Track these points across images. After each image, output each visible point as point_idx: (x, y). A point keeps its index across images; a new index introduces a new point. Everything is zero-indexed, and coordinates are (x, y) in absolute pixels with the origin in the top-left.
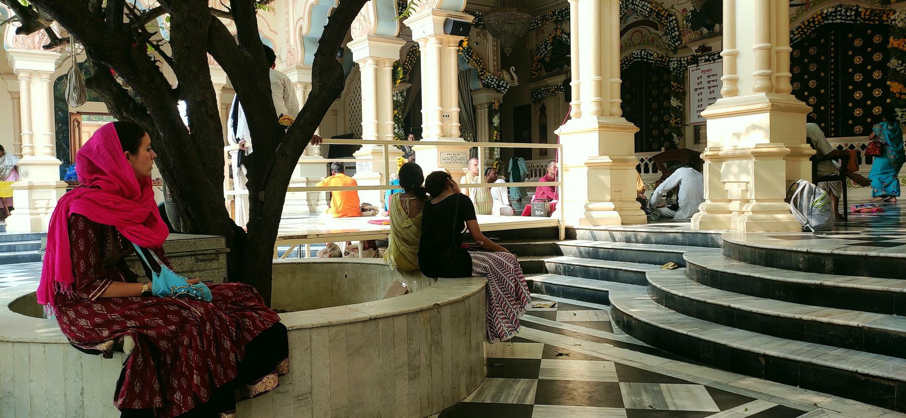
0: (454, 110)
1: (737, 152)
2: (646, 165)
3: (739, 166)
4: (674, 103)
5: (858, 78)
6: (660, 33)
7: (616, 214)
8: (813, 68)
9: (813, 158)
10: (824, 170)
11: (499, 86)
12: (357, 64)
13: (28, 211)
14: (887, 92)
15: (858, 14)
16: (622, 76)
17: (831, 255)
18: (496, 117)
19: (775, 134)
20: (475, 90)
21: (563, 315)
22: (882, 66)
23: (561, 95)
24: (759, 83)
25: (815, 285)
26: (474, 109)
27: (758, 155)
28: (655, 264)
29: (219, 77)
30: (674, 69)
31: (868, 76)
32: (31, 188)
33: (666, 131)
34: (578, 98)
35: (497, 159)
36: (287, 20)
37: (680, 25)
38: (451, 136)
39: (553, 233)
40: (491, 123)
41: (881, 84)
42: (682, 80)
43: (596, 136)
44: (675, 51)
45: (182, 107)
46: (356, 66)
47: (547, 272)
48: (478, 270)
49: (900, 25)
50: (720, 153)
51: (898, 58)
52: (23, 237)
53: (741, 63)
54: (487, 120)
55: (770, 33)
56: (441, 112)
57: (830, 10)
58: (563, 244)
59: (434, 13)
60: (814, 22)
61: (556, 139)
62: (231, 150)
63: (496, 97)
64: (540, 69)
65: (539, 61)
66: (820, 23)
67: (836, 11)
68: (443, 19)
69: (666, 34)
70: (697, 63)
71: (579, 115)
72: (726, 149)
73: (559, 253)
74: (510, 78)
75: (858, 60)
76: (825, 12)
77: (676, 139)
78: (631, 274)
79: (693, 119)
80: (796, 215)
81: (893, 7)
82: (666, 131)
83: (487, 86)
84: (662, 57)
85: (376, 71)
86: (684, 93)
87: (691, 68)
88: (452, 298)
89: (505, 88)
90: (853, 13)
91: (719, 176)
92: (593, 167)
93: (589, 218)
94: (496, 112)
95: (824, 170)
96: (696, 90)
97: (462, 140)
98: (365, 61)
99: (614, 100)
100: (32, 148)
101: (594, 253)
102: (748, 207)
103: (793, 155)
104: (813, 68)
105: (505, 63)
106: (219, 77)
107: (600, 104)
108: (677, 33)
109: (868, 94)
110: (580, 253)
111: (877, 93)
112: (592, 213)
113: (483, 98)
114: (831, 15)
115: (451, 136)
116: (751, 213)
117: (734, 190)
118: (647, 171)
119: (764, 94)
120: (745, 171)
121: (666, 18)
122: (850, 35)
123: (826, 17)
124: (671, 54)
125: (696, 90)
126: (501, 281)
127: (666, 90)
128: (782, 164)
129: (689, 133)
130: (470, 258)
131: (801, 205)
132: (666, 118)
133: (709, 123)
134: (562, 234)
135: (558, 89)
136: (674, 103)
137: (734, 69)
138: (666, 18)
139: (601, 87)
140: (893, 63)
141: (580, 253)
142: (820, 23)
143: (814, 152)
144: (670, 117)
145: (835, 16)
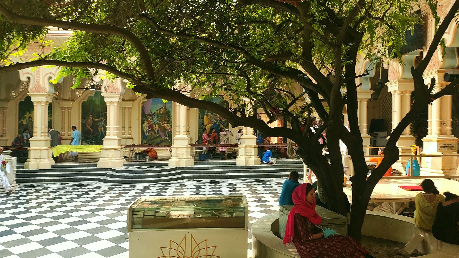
0: (449, 120)
12: (391, 93)
13: (244, 157)
29: (343, 147)
32: (246, 147)
45: (329, 163)
52: (242, 167)
59: (438, 71)
62: (347, 176)
68: (444, 73)
97: (453, 137)
98: (395, 92)
100: (246, 131)
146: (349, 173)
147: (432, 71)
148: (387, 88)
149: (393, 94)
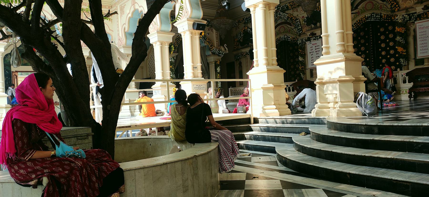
1: (331, 80)
2: (289, 88)
3: (332, 87)
4: (301, 59)
5: (383, 45)
6: (293, 27)
7: (277, 111)
8: (362, 41)
9: (365, 82)
10: (371, 87)
11: (219, 53)
14: (396, 51)
15: (381, 17)
16: (277, 47)
17: (377, 126)
18: (218, 68)
19: (348, 71)
20: (208, 55)
21: (254, 159)
22: (393, 40)
23: (248, 57)
24: (339, 48)
25: (370, 140)
26: (208, 64)
27: (340, 81)
28: (296, 133)
29: (86, 51)
30: (300, 43)
31: (387, 45)
33: (297, 72)
34: (257, 58)
35: (220, 88)
36: (118, 25)
37: (302, 23)
38: (198, 77)
39: (248, 120)
40: (216, 71)
41: (393, 48)
42: (304, 48)
43: (266, 75)
44: (300, 35)
45: (69, 66)
46: (152, 45)
47: (246, 139)
48: (214, 139)
49: (400, 21)
50: (323, 81)
51: (400, 36)
53: (331, 39)
54: (214, 69)
55: (343, 25)
56: (193, 66)
57: (369, 15)
58: (253, 126)
60: (362, 21)
61: (247, 77)
62: (93, 86)
63: (218, 59)
64: (238, 45)
65: (237, 41)
66: (364, 21)
67: (371, 16)
68: (193, 22)
69: (295, 28)
70: (310, 41)
71: (258, 65)
72: (326, 79)
73: (251, 130)
74: (225, 50)
75: (382, 37)
76: (367, 16)
77: (302, 76)
78: (285, 138)
79: (309, 66)
80: (359, 108)
81: (397, 13)
82: (297, 72)
83: (214, 54)
84: (294, 38)
85: (161, 47)
86: (305, 54)
87: (308, 43)
88: (203, 152)
89: (222, 54)
90: (379, 16)
91: (323, 91)
92: (265, 89)
93: (265, 113)
94: (218, 65)
95: (371, 87)
96: (310, 53)
97: (203, 78)
98: (156, 43)
99: (273, 58)
101: (268, 130)
102: (337, 106)
103: (356, 81)
104: (362, 41)
105: (222, 43)
106: (86, 51)
107: (267, 60)
108: (300, 27)
109: (388, 53)
110: (261, 129)
111: (392, 52)
112: (267, 111)
113: (212, 59)
114: (369, 17)
115: (198, 77)
116: (339, 108)
117: (330, 98)
118: (289, 91)
119: (341, 53)
120: (335, 88)
121: (295, 21)
122: (378, 26)
123: (368, 18)
124: (298, 37)
125: (310, 53)
126: (225, 144)
127: (296, 53)
128: (351, 85)
129: (308, 73)
130: (210, 133)
131: (361, 104)
132: (297, 66)
133: (318, 67)
134: (252, 121)
135: (247, 54)
136: (301, 59)
137: (327, 43)
138: (295, 21)
139: (267, 52)
140: (398, 38)
141: (261, 129)
142: (364, 21)
143: (366, 79)
144: (299, 65)
145: (371, 18)
146: (96, 82)
147: (183, 20)
148: (149, 40)
149: (154, 45)
